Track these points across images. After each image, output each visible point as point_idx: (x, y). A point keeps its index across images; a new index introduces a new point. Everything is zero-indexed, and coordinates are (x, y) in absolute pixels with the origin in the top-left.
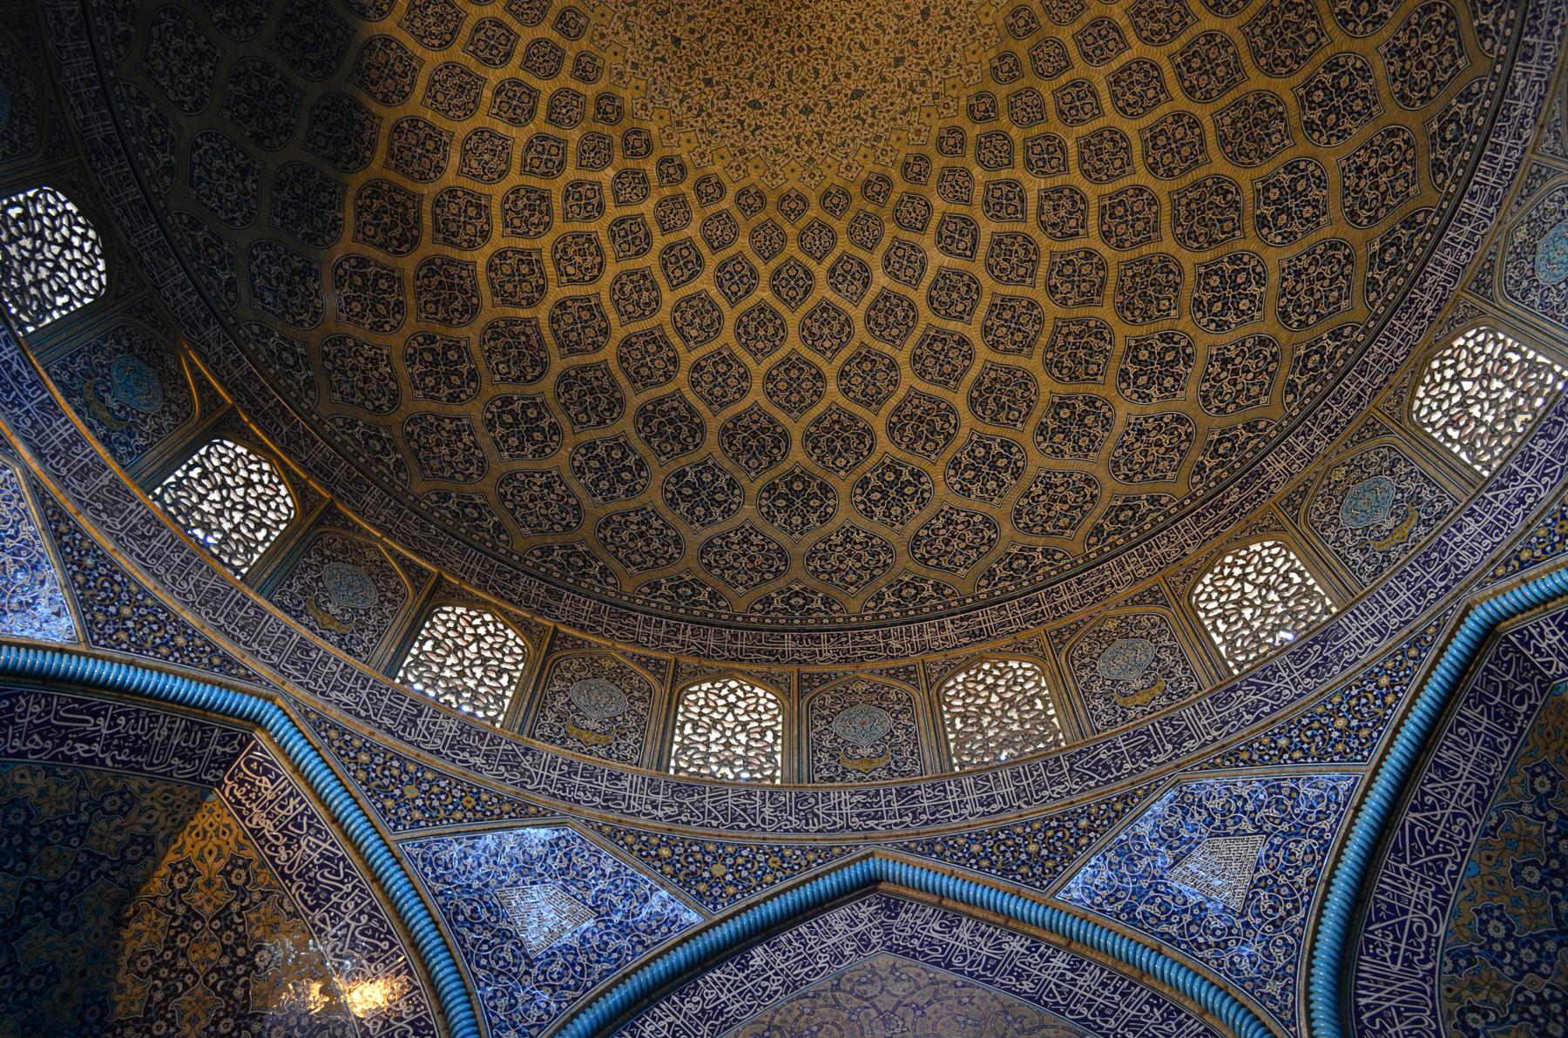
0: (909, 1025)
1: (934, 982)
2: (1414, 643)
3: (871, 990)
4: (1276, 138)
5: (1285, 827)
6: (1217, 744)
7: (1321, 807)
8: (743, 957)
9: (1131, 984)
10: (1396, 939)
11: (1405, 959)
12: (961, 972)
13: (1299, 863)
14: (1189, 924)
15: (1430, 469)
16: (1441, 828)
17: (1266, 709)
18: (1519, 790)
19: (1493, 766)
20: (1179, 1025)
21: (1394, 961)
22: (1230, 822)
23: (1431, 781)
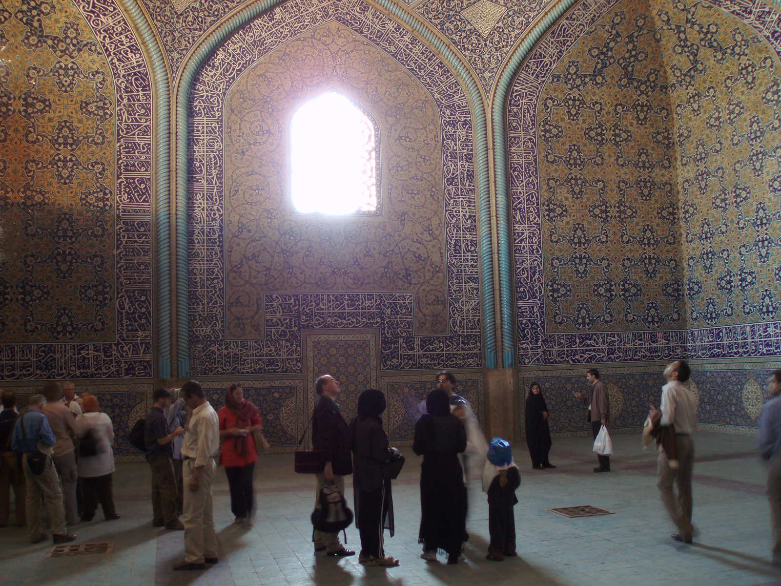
0: (343, 61)
1: (355, 41)
3: (329, 41)
5: (516, 8)
7: (533, 6)
8: (271, 13)
9: (433, 55)
10: (537, 67)
11: (537, 75)
12: (366, 37)
13: (515, 27)
14: (464, 38)
16: (572, 28)
18: (608, 20)
19: (604, 9)
20: (447, 78)
21: (533, 74)
23: (579, 9)
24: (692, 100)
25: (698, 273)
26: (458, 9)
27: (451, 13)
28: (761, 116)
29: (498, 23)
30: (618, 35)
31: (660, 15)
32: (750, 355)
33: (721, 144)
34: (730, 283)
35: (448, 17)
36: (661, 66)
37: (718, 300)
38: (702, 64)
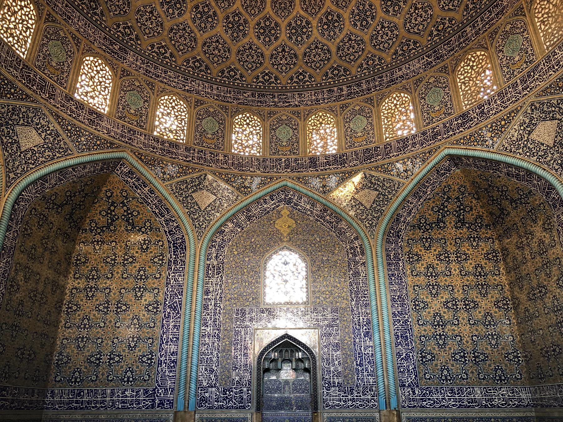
2: (111, 143)
4: (223, 5)
5: (50, 145)
6: (58, 110)
7: (61, 150)
14: (9, 143)
15: (150, 115)
17: (74, 116)
22: (41, 130)
24: (95, 243)
25: (71, 350)
26: (15, 123)
27: (10, 122)
28: (147, 268)
29: (35, 147)
30: (83, 191)
31: (107, 192)
32: (106, 409)
33: (112, 275)
34: (99, 360)
35: (7, 123)
36: (85, 217)
37: (85, 370)
38: (115, 227)
